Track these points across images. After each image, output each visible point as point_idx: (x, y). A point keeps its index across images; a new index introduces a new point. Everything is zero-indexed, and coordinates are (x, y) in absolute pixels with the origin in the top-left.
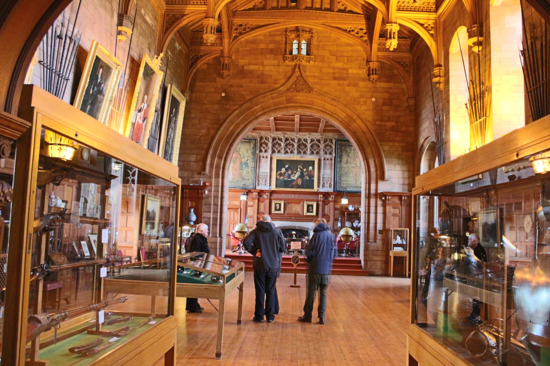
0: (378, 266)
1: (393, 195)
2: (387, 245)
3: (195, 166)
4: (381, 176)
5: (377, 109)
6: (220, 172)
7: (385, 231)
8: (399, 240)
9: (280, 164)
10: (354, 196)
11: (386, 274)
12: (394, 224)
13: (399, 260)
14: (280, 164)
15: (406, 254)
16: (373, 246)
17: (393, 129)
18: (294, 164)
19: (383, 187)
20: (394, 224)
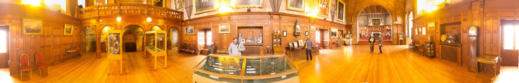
0: (396, 42)
1: (399, 24)
2: (398, 37)
3: (350, 20)
4: (396, 20)
5: (394, 2)
6: (356, 21)
7: (397, 34)
8: (401, 36)
9: (373, 20)
10: (389, 26)
11: (398, 44)
12: (399, 32)
13: (401, 41)
14: (373, 20)
15: (403, 39)
16: (394, 37)
17: (399, 8)
18: (376, 20)
19: (397, 23)
20: (399, 32)
